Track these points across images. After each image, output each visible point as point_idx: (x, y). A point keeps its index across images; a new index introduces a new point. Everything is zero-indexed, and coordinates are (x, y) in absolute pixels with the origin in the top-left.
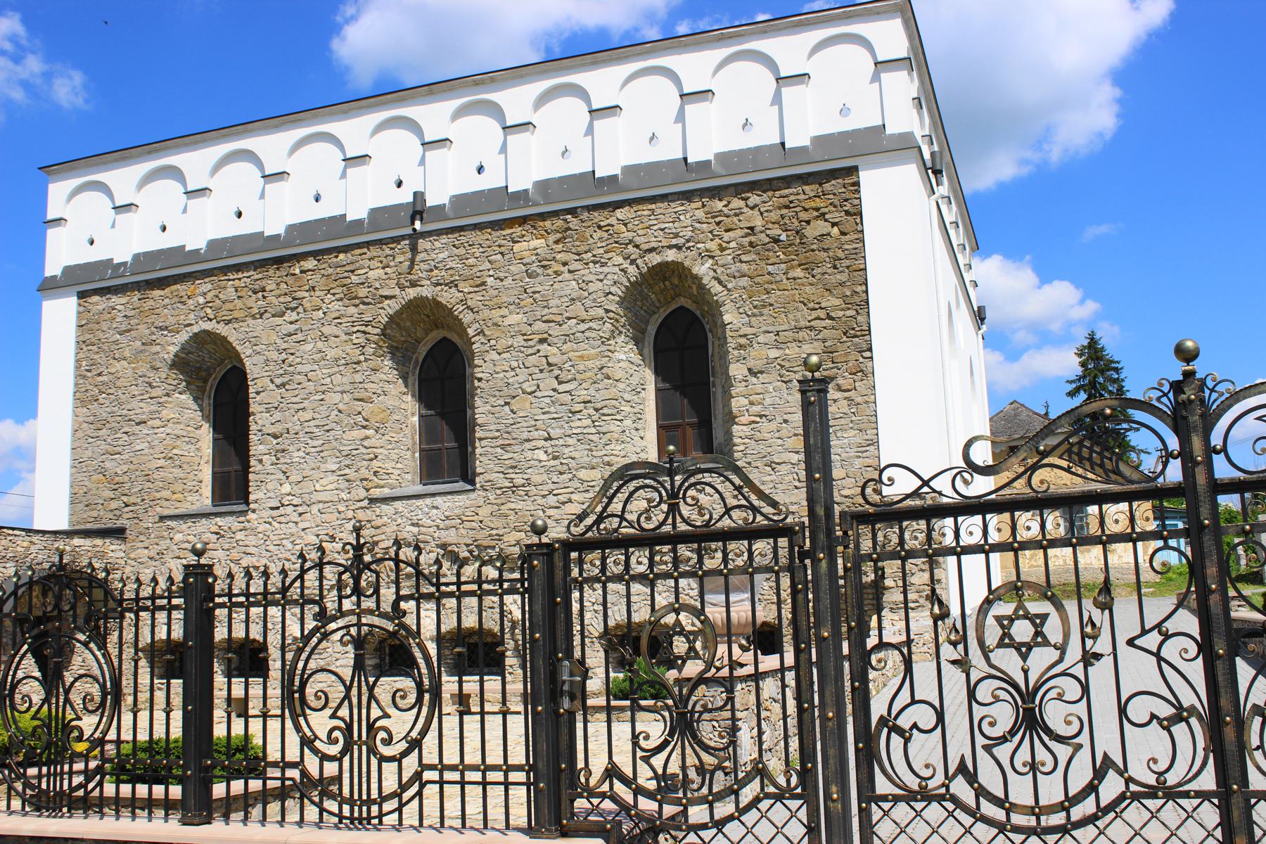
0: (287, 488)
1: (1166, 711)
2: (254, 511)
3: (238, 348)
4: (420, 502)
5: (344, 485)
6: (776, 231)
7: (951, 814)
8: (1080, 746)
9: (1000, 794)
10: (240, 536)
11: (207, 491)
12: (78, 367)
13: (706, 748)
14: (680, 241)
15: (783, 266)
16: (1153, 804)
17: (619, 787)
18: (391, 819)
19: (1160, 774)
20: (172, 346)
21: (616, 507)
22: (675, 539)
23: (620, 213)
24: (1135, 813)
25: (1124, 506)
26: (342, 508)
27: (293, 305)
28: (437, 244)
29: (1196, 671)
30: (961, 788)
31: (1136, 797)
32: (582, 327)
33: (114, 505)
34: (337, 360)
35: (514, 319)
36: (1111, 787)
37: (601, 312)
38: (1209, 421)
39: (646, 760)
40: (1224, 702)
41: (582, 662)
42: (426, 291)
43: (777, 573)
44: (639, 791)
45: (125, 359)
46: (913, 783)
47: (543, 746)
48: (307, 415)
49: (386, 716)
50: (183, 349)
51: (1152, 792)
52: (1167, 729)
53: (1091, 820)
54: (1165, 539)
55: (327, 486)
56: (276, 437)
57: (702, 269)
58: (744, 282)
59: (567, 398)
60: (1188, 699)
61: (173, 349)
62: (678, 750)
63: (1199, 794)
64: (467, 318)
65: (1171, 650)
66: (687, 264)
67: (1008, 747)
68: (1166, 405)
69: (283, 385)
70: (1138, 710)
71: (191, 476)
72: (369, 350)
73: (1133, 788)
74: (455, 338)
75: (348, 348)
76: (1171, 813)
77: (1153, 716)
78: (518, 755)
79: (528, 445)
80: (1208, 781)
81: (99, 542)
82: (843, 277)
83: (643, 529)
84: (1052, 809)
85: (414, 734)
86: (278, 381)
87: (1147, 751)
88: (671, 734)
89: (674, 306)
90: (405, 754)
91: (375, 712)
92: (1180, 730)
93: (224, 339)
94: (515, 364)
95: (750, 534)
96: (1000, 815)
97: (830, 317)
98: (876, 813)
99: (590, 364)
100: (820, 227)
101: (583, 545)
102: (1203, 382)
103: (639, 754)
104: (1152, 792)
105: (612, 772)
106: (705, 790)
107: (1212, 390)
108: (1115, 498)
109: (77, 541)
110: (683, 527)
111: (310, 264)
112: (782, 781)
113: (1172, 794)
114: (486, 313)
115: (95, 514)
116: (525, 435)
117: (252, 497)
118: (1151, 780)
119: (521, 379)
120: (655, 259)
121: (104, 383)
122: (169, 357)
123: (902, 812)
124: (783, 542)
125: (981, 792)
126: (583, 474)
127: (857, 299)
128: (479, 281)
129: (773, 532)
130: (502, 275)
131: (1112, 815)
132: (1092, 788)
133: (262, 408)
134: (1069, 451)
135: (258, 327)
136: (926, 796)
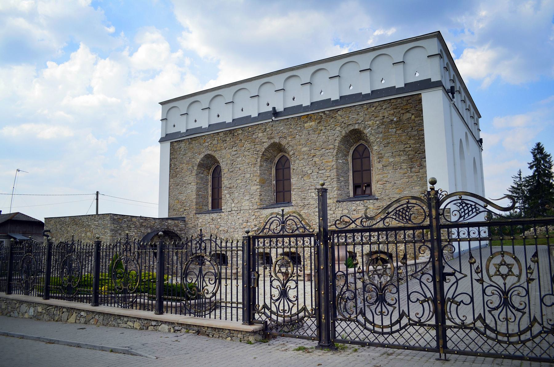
0: (233, 205)
1: (422, 298)
2: (223, 212)
5: (251, 204)
6: (391, 118)
7: (357, 326)
8: (396, 307)
9: (372, 320)
10: (219, 220)
11: (210, 206)
13: (291, 301)
14: (360, 121)
15: (395, 129)
16: (417, 327)
17: (266, 311)
18: (208, 316)
19: (419, 318)
20: (198, 159)
21: (267, 226)
22: (283, 236)
23: (339, 112)
24: (411, 330)
25: (411, 232)
26: (250, 211)
28: (280, 125)
29: (431, 285)
30: (360, 318)
31: (411, 325)
33: (182, 210)
36: (405, 321)
38: (439, 203)
39: (274, 303)
40: (438, 297)
41: (258, 272)
42: (277, 140)
43: (311, 248)
44: (272, 312)
46: (348, 316)
47: (246, 297)
48: (239, 181)
49: (207, 285)
50: (202, 160)
51: (416, 323)
52: (422, 304)
53: (398, 331)
54: (424, 243)
55: (246, 204)
56: (230, 188)
57: (367, 131)
58: (381, 136)
59: (322, 175)
60: (429, 295)
61: (198, 160)
62: (282, 300)
63: (429, 325)
64: (290, 149)
65: (424, 279)
66: (362, 129)
67: (375, 306)
68: (425, 199)
69: (232, 171)
70: (413, 297)
71: (205, 201)
72: (259, 160)
73: (411, 322)
74: (287, 155)
76: (422, 330)
77: (418, 300)
78: (240, 300)
79: (310, 191)
80: (433, 322)
81: (176, 222)
82: (416, 133)
83: (274, 233)
84: (387, 327)
85: (214, 291)
87: (416, 310)
88: (280, 296)
89: (359, 144)
90: (212, 297)
91: (204, 284)
92: (426, 304)
93: (214, 157)
94: (305, 164)
95: (303, 236)
96: (371, 327)
97: (410, 147)
98: (337, 324)
99: (329, 164)
100: (408, 115)
101: (258, 237)
102: (437, 191)
103: (272, 301)
104: (416, 323)
105: (265, 306)
106: (289, 314)
107: (440, 194)
108: (409, 228)
109: (170, 221)
110: (286, 233)
111: (240, 132)
112: (310, 312)
113: (422, 325)
115: (176, 213)
116: (308, 188)
117: (223, 208)
118: (417, 320)
120: (352, 128)
122: (197, 163)
123: (344, 324)
124: (312, 239)
125: (366, 320)
127: (421, 141)
128: (293, 136)
129: (310, 235)
130: (301, 134)
131: (404, 330)
132: (398, 322)
134: (396, 213)
136: (350, 320)
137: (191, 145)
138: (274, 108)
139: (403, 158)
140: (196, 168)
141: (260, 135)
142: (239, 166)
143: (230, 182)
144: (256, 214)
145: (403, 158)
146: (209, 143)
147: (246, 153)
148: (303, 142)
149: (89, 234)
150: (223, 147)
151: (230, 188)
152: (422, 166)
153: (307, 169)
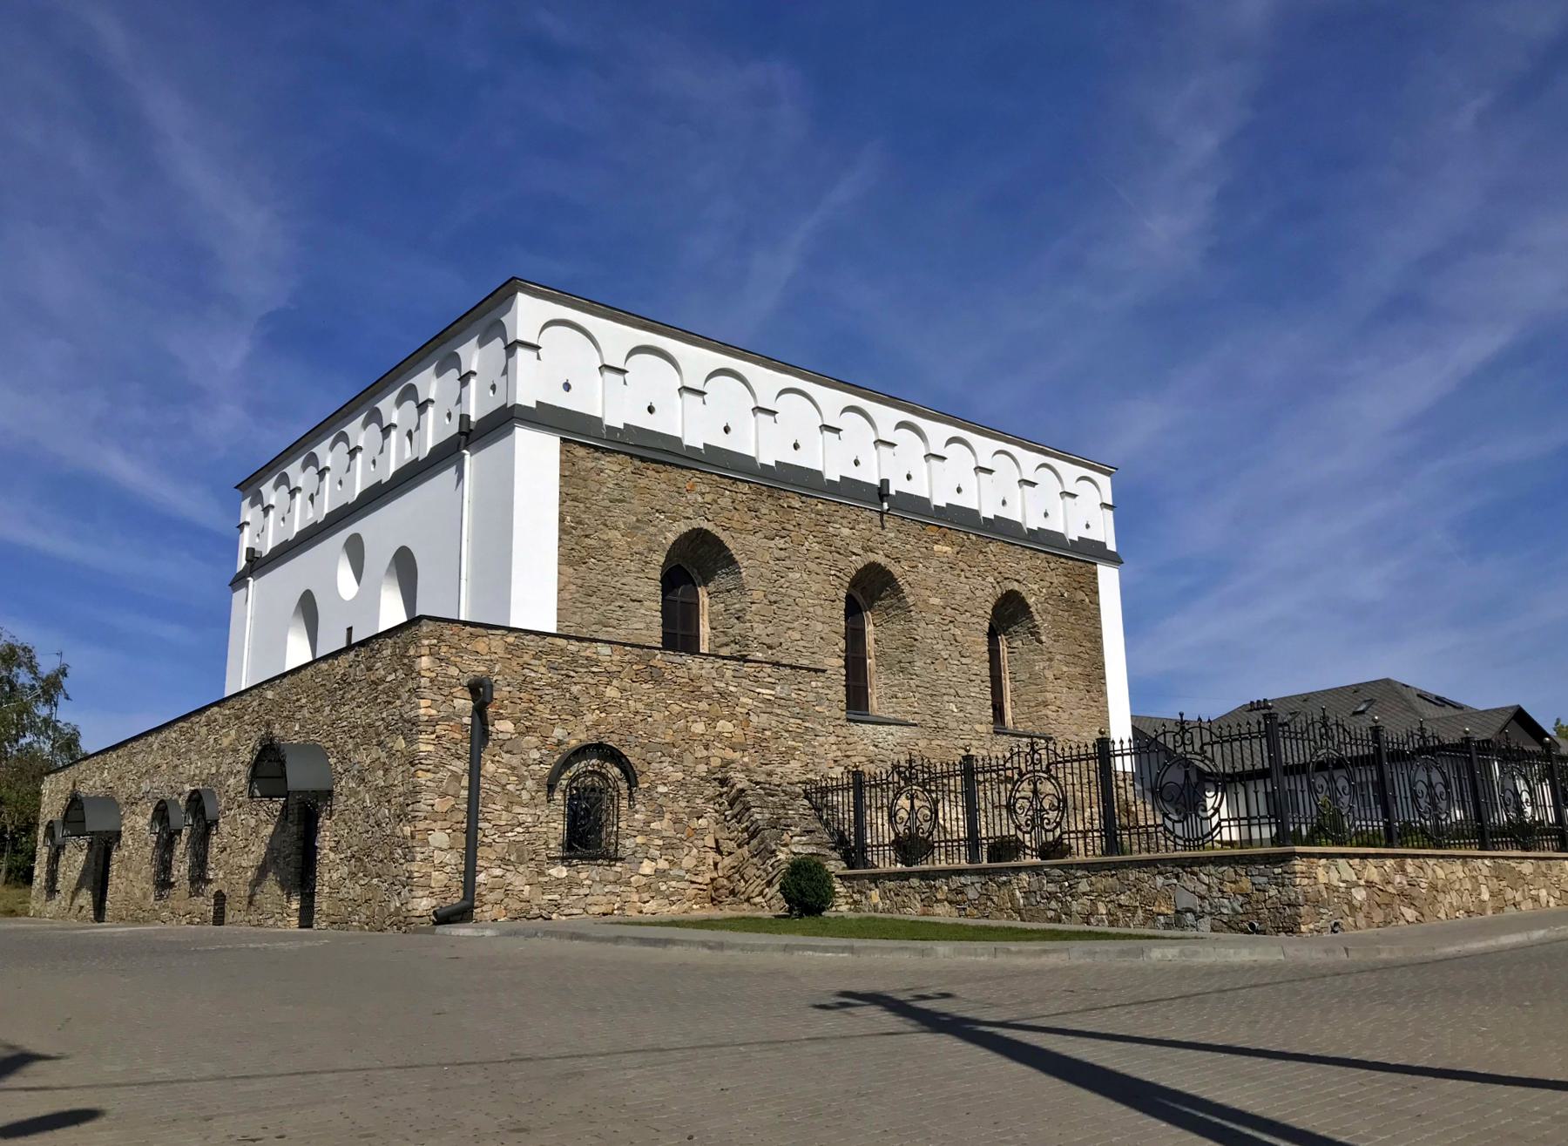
3: (737, 558)
4: (880, 728)
12: (562, 520)
27: (783, 533)
32: (974, 620)
34: (819, 594)
35: (935, 601)
37: (981, 612)
42: (880, 559)
45: (617, 528)
56: (770, 647)
57: (1031, 600)
61: (672, 537)
64: (907, 589)
75: (828, 587)
86: (773, 598)
100: (1080, 595)
114: (918, 591)
119: (940, 647)
121: (590, 547)
126: (977, 727)
133: (757, 618)
135: (755, 541)
137: (643, 482)
138: (885, 483)
139: (1079, 670)
140: (660, 558)
141: (846, 532)
142: (795, 593)
143: (770, 630)
144: (839, 731)
145: (1079, 670)
146: (708, 498)
147: (812, 566)
148: (931, 583)
149: (724, 726)
150: (750, 527)
151: (770, 647)
152: (1103, 693)
153: (940, 647)
